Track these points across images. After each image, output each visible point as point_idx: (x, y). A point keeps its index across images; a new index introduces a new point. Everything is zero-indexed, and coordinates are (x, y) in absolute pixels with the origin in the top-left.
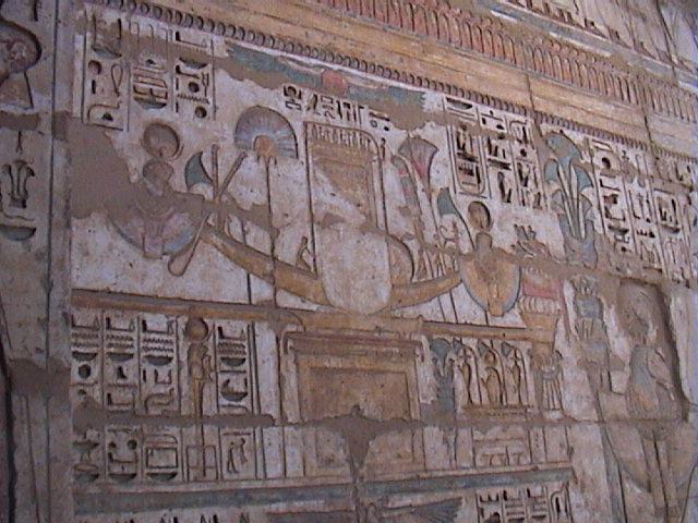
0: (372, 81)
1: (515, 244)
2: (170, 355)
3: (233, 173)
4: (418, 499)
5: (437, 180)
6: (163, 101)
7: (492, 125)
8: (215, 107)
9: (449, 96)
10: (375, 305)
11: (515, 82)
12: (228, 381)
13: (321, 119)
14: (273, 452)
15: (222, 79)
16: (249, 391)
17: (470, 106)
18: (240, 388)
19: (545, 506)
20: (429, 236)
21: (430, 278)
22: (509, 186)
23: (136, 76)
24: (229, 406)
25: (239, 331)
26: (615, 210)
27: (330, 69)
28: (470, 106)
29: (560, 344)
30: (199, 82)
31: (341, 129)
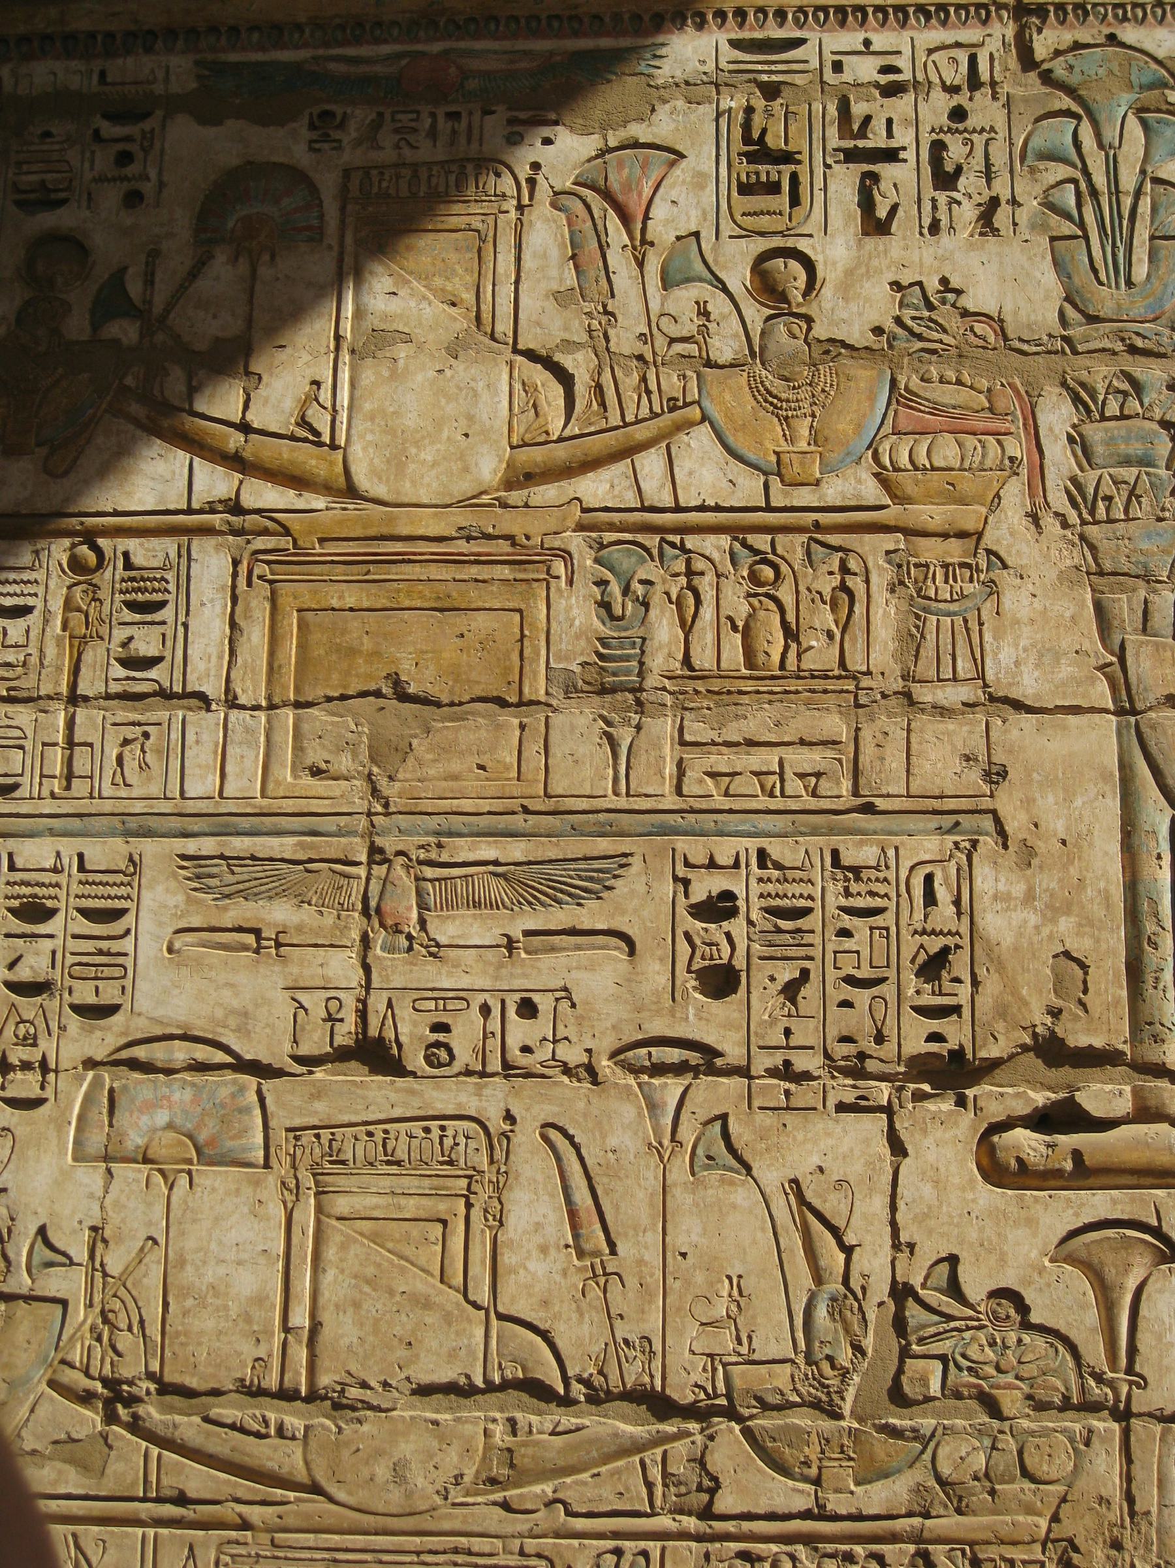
0: (525, 52)
1: (889, 325)
2: (30, 601)
3: (181, 291)
4: (517, 850)
5: (667, 222)
6: (63, 195)
7: (865, 69)
8: (161, 185)
9: (733, 36)
10: (463, 487)
12: (131, 639)
13: (387, 155)
14: (201, 756)
15: (183, 135)
16: (168, 654)
17: (801, 42)
18: (152, 651)
19: (881, 888)
20: (624, 340)
21: (615, 420)
22: (893, 197)
23: (19, 164)
24: (128, 678)
25: (161, 556)
27: (423, 54)
28: (801, 42)
30: (133, 148)
31: (429, 165)
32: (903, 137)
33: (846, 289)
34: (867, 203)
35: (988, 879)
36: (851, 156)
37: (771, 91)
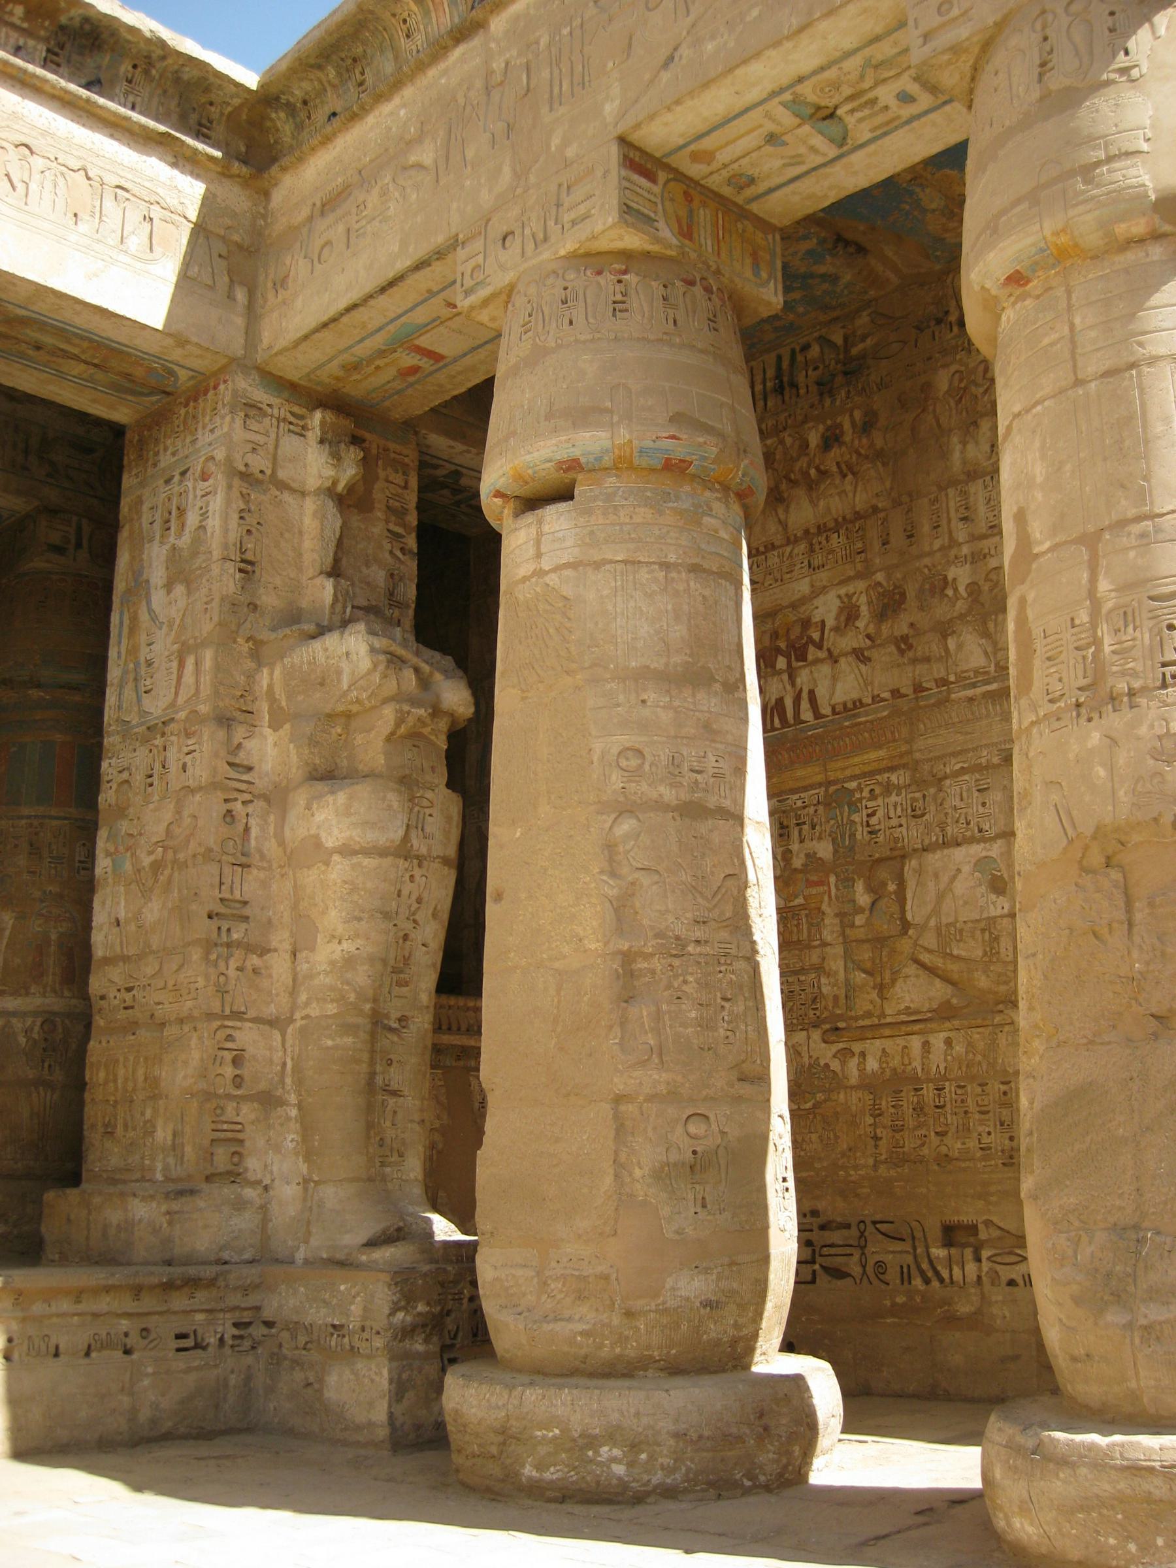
11: (817, 770)
26: (873, 821)
29: (824, 907)
32: (806, 819)
33: (797, 857)
34: (800, 835)
35: (824, 980)
36: (798, 825)
37: (784, 812)
